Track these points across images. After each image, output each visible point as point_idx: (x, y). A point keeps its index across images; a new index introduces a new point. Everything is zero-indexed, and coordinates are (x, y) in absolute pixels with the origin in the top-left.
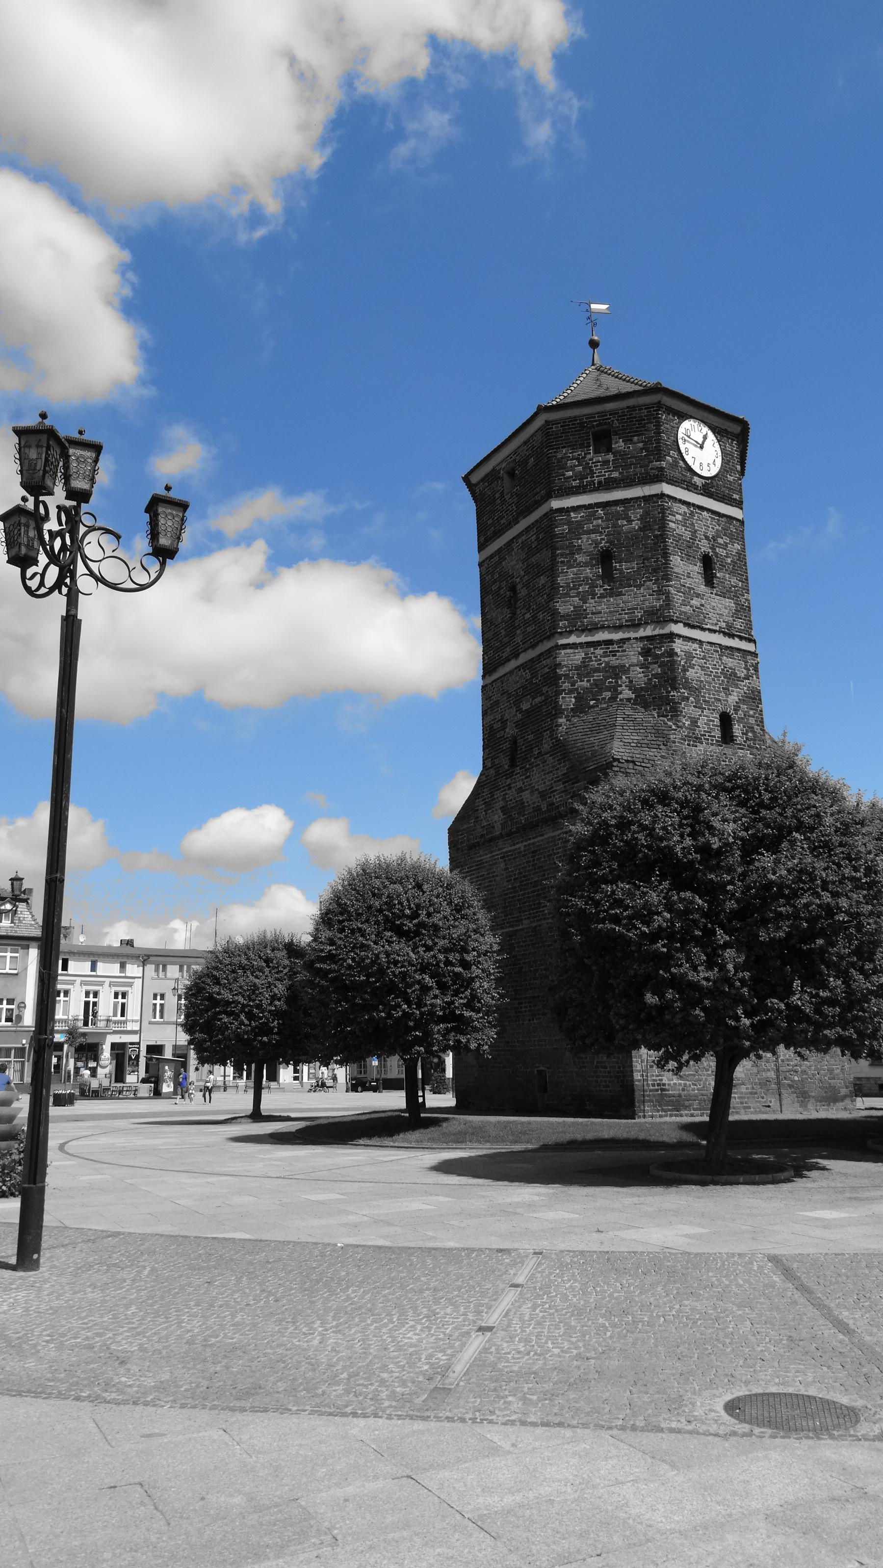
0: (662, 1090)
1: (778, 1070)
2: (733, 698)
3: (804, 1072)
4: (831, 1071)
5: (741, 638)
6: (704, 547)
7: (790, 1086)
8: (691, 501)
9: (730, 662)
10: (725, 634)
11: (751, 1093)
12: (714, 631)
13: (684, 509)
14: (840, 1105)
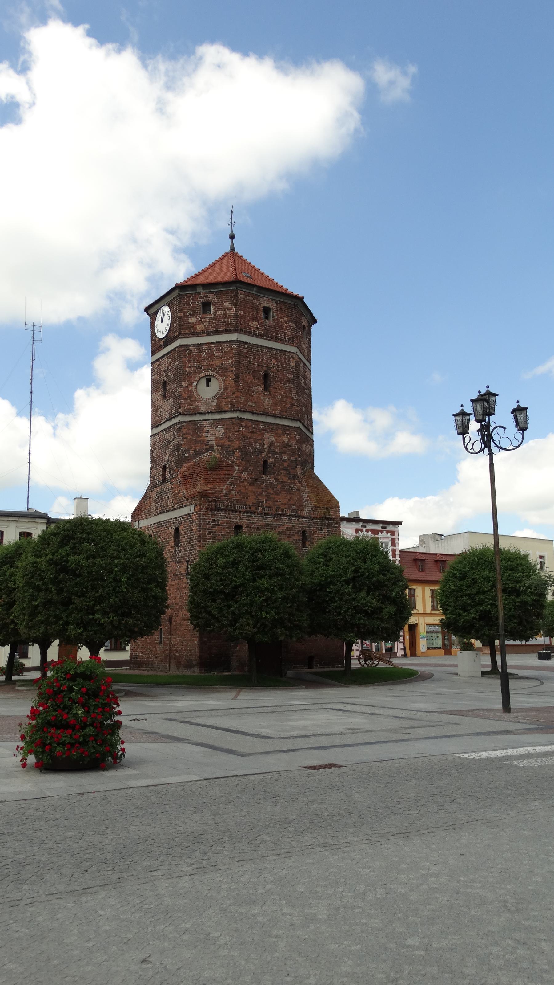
0: (137, 658)
1: (170, 650)
2: (168, 455)
3: (180, 651)
4: (190, 650)
5: (174, 417)
6: (164, 378)
7: (175, 658)
8: (159, 357)
9: (167, 436)
10: (168, 420)
11: (161, 661)
12: (164, 422)
13: (158, 363)
14: (192, 670)
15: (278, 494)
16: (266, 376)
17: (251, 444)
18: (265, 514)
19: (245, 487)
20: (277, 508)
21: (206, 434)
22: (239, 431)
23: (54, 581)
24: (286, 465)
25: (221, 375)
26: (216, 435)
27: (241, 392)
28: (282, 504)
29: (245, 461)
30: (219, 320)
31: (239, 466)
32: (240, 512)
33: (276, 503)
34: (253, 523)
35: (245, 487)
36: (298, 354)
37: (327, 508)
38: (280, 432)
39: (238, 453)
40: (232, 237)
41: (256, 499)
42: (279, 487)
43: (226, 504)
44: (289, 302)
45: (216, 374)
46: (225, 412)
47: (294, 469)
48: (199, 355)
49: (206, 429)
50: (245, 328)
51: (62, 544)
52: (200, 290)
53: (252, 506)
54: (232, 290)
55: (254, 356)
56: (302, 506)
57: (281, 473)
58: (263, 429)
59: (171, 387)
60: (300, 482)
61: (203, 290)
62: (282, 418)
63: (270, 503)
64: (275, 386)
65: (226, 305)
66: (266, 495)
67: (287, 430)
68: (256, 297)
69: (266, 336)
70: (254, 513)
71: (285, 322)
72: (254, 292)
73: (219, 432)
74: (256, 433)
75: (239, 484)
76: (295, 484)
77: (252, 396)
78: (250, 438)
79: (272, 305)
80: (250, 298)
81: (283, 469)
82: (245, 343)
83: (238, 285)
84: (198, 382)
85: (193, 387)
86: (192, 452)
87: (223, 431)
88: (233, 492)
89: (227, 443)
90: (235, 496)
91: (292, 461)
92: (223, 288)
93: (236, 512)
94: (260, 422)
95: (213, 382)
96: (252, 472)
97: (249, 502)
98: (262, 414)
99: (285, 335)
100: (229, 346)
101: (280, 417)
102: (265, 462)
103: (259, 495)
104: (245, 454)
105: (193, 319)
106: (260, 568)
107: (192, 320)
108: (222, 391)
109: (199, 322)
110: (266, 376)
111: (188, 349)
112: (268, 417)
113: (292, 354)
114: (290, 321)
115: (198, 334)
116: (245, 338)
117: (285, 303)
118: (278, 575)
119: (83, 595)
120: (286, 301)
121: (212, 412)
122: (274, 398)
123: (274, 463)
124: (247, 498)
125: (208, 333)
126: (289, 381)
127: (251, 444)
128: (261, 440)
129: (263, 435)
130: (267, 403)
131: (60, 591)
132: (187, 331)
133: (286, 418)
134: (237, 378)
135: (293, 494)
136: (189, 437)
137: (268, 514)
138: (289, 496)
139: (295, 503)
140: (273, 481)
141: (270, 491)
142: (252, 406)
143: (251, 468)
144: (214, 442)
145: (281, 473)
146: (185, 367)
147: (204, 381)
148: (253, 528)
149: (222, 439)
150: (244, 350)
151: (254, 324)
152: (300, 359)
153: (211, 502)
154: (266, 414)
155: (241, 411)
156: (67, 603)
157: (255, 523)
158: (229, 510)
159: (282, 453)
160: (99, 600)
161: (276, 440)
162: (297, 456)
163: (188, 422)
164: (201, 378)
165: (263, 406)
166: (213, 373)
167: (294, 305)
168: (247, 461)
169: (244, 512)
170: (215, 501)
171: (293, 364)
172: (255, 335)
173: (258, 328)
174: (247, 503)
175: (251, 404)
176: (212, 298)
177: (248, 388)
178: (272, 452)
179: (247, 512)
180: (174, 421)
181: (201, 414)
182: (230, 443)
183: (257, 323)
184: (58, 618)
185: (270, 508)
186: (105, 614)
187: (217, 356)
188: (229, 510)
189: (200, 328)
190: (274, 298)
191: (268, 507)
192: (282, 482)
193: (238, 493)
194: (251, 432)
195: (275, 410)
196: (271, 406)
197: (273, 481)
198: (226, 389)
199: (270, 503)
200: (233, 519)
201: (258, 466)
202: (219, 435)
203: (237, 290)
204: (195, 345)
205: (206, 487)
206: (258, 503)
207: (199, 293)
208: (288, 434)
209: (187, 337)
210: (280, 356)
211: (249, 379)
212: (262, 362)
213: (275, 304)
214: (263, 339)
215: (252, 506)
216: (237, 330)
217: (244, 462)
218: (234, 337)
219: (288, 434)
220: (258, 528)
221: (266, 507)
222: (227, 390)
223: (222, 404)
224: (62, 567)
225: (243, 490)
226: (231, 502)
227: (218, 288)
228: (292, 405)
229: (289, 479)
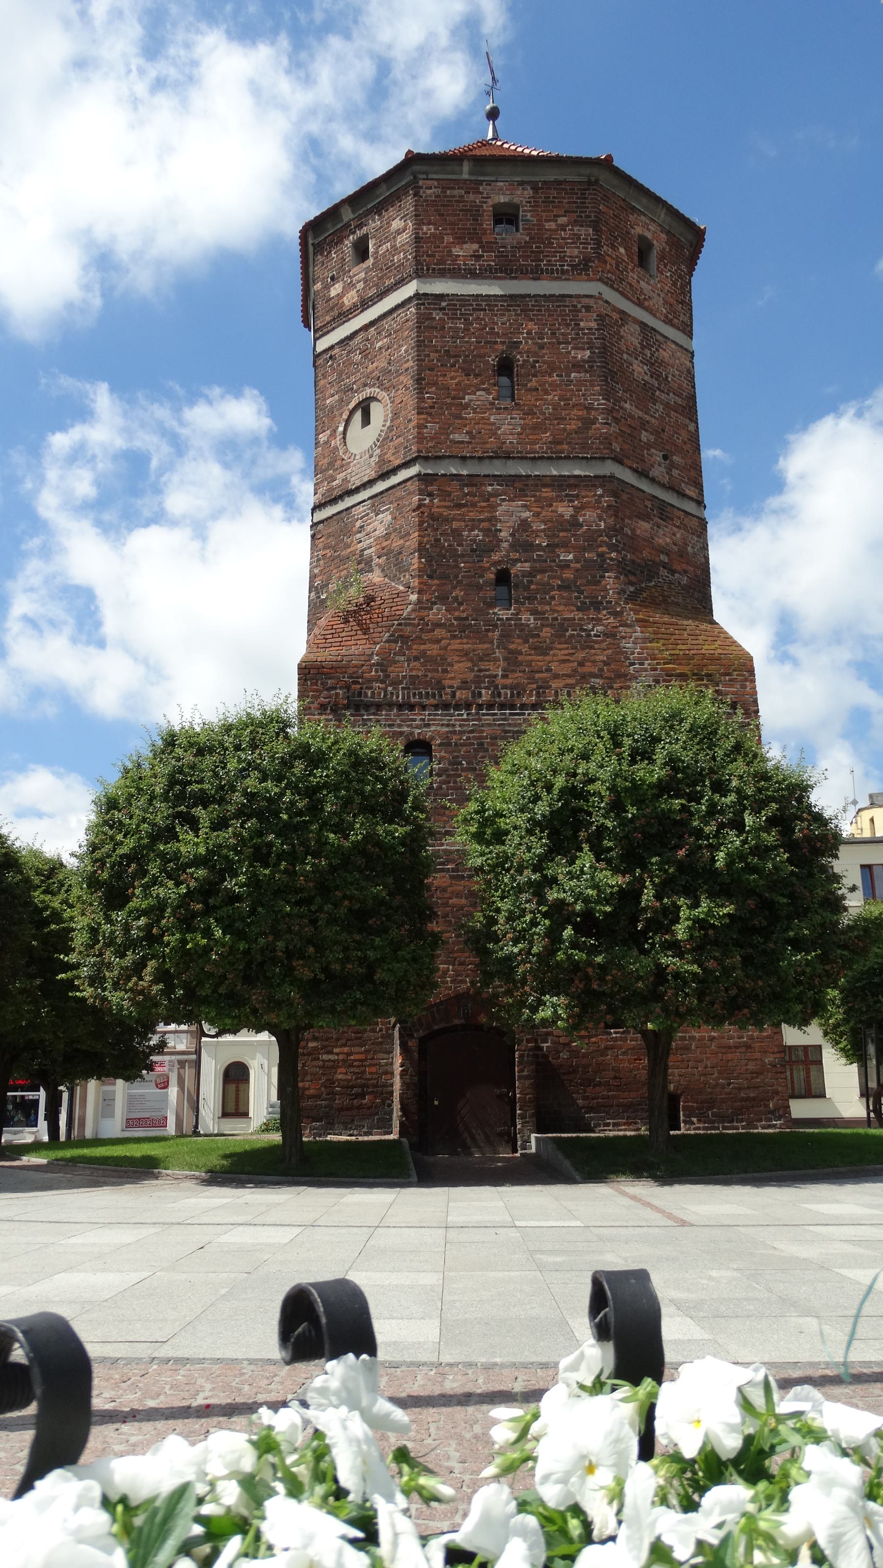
15: (542, 650)
17: (457, 533)
18: (502, 706)
19: (438, 641)
20: (539, 687)
21: (359, 536)
22: (419, 506)
24: (568, 575)
25: (387, 389)
26: (377, 533)
27: (430, 414)
28: (556, 676)
29: (439, 578)
30: (384, 267)
31: (419, 593)
32: (424, 708)
33: (537, 676)
34: (463, 732)
35: (438, 641)
36: (606, 296)
37: (708, 675)
38: (547, 493)
39: (415, 562)
41: (472, 670)
42: (546, 633)
43: (376, 691)
44: (570, 178)
45: (378, 390)
46: (394, 471)
47: (596, 582)
48: (349, 363)
49: (358, 524)
50: (442, 262)
52: (347, 215)
53: (459, 688)
54: (407, 186)
55: (468, 323)
56: (625, 675)
57: (553, 598)
58: (495, 494)
60: (615, 614)
61: (354, 212)
62: (556, 458)
63: (516, 677)
64: (533, 383)
66: (505, 659)
67: (570, 486)
68: (473, 186)
69: (506, 269)
70: (468, 706)
71: (563, 228)
72: (465, 176)
73: (380, 523)
74: (474, 505)
75: (419, 637)
76: (598, 621)
77: (462, 418)
78: (453, 519)
79: (522, 196)
80: (456, 192)
81: (559, 587)
82: (441, 297)
83: (416, 168)
84: (348, 422)
85: (338, 438)
86: (332, 587)
87: (389, 518)
88: (402, 658)
89: (397, 543)
90: (403, 669)
91: (588, 565)
92: (388, 190)
93: (412, 707)
94: (488, 476)
95: (378, 412)
96: (461, 604)
97: (451, 681)
98: (491, 458)
99: (562, 259)
100: (401, 314)
101: (550, 458)
103: (481, 660)
104: (439, 563)
105: (337, 286)
107: (336, 290)
108: (388, 424)
111: (331, 357)
112: (510, 463)
113: (587, 300)
114: (575, 223)
115: (344, 316)
116: (439, 287)
117: (559, 183)
120: (561, 178)
121: (371, 483)
122: (531, 413)
123: (531, 574)
124: (445, 671)
125: (364, 304)
126: (577, 366)
127: (457, 533)
128: (489, 520)
129: (493, 508)
130: (508, 427)
132: (328, 318)
133: (567, 458)
134: (419, 380)
135: (592, 648)
136: (329, 552)
137: (512, 707)
138: (580, 655)
139: (601, 670)
140: (528, 619)
142: (462, 442)
143: (458, 593)
144: (373, 549)
145: (553, 598)
146: (325, 400)
147: (358, 416)
148: (462, 745)
149: (387, 536)
150: (437, 315)
152: (622, 312)
153: (335, 688)
155: (426, 458)
157: (471, 732)
158: (391, 705)
159: (557, 546)
161: (537, 515)
162: (604, 549)
163: (326, 519)
164: (352, 413)
165: (498, 438)
166: (372, 389)
167: (589, 183)
168: (443, 577)
169: (436, 707)
170: (348, 688)
172: (472, 274)
173: (478, 257)
174: (446, 682)
175: (457, 437)
177: (448, 401)
179: (446, 706)
181: (350, 493)
182: (402, 542)
183: (475, 246)
185: (518, 690)
187: (380, 348)
188: (391, 705)
190: (526, 178)
191: (512, 688)
192: (556, 619)
193: (416, 659)
194: (459, 506)
195: (534, 443)
196: (519, 434)
197: (528, 619)
198: (396, 415)
199: (516, 677)
200: (400, 726)
201: (480, 588)
202: (381, 531)
203: (416, 179)
204: (341, 342)
206: (478, 681)
207: (347, 225)
208: (577, 496)
209: (328, 332)
210: (548, 310)
211: (453, 378)
212: (492, 332)
213: (529, 192)
214: (495, 278)
215: (459, 688)
216: (420, 273)
217: (436, 582)
218: (410, 289)
219: (577, 496)
220: (482, 744)
221: (505, 687)
222: (398, 417)
223: (389, 456)
225: (433, 650)
226: (395, 683)
227: (378, 197)
228: (588, 423)
229: (579, 609)
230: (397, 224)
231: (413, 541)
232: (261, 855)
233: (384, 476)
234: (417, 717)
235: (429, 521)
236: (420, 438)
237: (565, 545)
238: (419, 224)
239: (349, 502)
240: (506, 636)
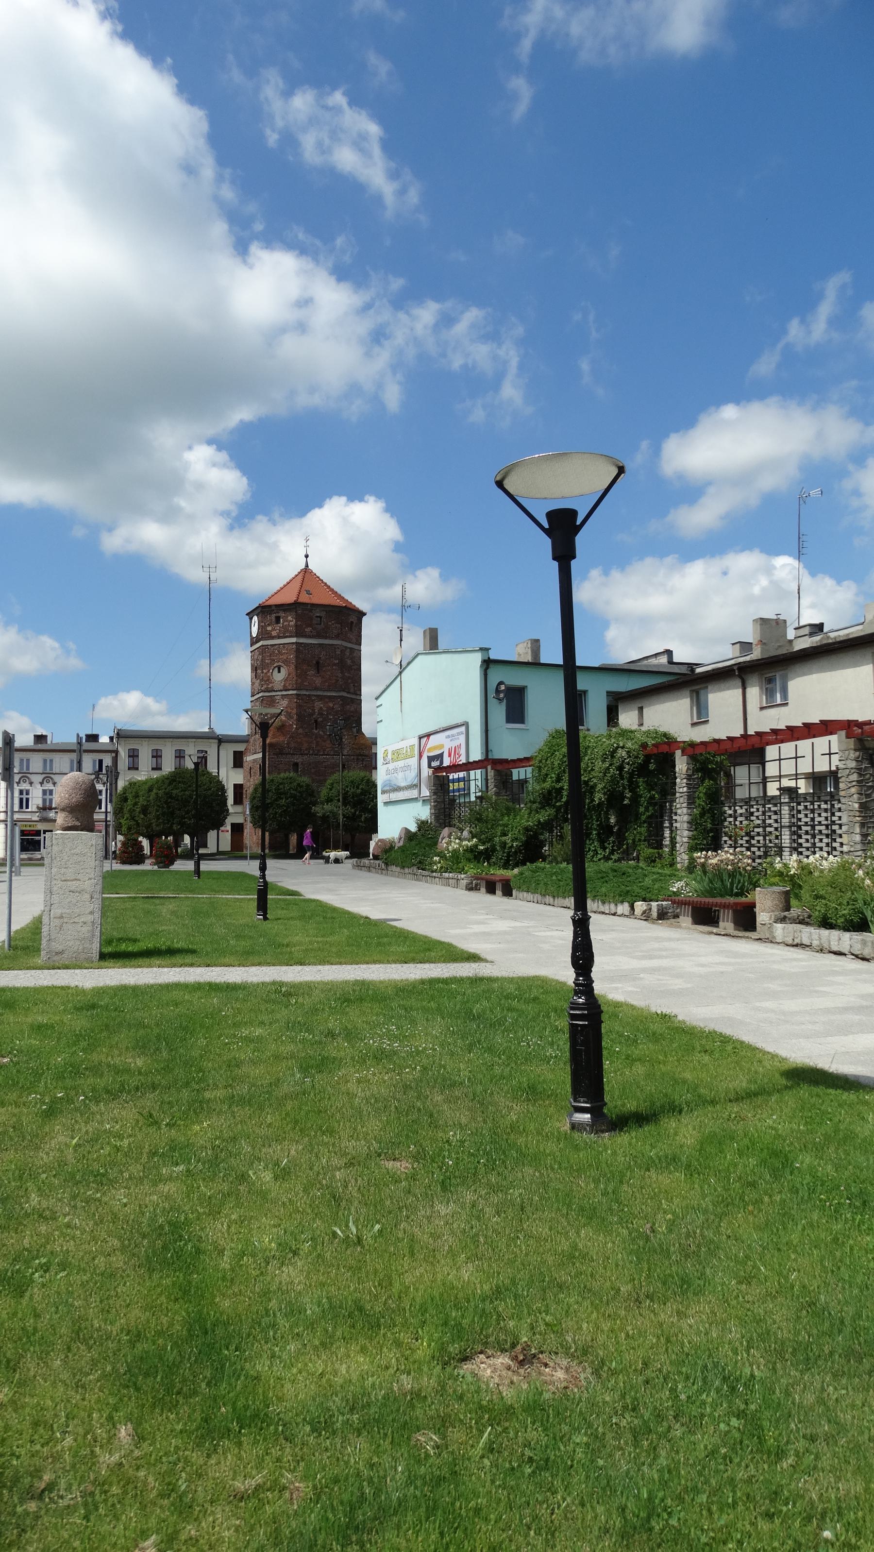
16: (318, 663)
23: (166, 802)
38: (327, 700)
40: (307, 556)
43: (286, 750)
46: (289, 690)
48: (274, 652)
51: (170, 784)
52: (274, 608)
59: (259, 671)
65: (290, 618)
68: (311, 611)
73: (285, 703)
79: (323, 614)
90: (293, 745)
102: (316, 721)
104: (300, 718)
106: (281, 794)
107: (269, 628)
109: (273, 629)
110: (318, 663)
115: (273, 638)
116: (302, 640)
118: (291, 797)
119: (179, 810)
121: (281, 691)
125: (279, 637)
126: (335, 665)
130: (318, 681)
131: (169, 808)
134: (296, 667)
141: (319, 739)
147: (276, 669)
151: (308, 630)
154: (316, 689)
156: (172, 813)
160: (187, 812)
171: (338, 652)
176: (282, 614)
178: (321, 714)
180: (260, 695)
184: (169, 821)
185: (319, 751)
186: (190, 819)
189: (274, 633)
198: (289, 674)
202: (285, 705)
205: (274, 740)
216: (296, 636)
218: (294, 640)
224: (169, 795)
225: (299, 740)
230: (290, 618)
231: (295, 711)
232: (293, 804)
233: (286, 690)
234: (296, 757)
235: (299, 706)
236: (296, 684)
237: (330, 714)
238: (296, 622)
239: (274, 694)
240: (316, 737)
